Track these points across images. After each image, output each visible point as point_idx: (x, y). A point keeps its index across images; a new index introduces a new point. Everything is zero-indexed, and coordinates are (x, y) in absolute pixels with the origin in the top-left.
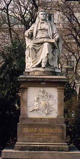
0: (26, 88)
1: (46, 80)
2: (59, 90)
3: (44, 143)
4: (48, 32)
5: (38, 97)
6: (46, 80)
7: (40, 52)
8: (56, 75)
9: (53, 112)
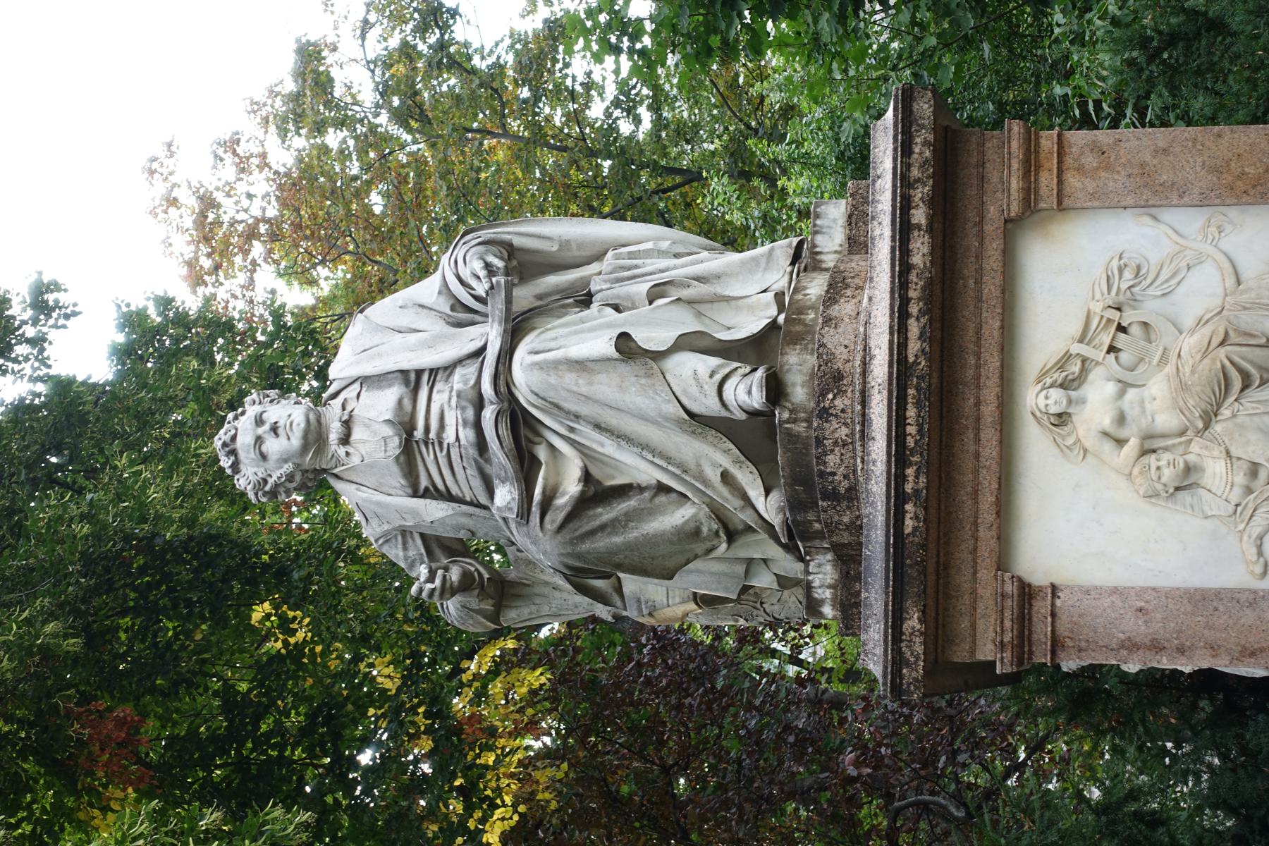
0: (1027, 592)
1: (914, 347)
4: (434, 372)
7: (608, 447)
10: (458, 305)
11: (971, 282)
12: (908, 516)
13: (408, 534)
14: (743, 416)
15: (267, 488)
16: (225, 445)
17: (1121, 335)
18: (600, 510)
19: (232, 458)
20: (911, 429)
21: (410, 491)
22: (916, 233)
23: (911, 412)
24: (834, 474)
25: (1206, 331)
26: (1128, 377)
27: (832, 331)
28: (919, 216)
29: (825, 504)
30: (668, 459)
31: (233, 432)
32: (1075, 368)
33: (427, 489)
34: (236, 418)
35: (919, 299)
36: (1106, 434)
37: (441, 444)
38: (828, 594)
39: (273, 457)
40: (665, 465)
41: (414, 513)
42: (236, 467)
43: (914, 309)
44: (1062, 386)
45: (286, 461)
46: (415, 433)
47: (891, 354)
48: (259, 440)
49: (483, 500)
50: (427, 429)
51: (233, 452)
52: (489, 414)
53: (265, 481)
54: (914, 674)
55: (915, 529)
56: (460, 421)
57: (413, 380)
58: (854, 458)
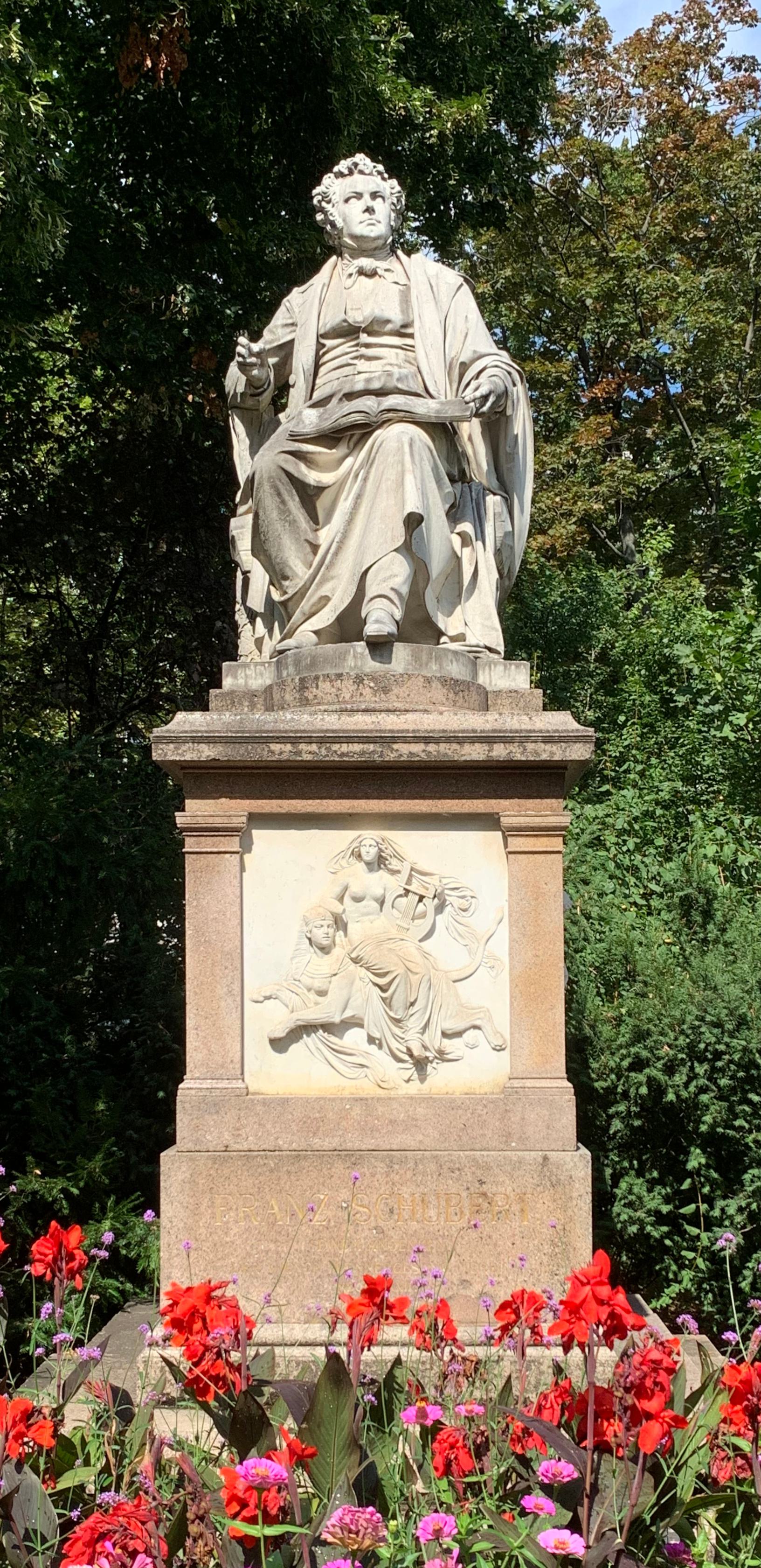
5: (338, 908)
7: (344, 506)
11: (454, 789)
12: (282, 746)
13: (293, 328)
14: (363, 615)
15: (324, 204)
16: (356, 165)
17: (417, 898)
18: (297, 499)
19: (346, 172)
21: (322, 331)
22: (487, 748)
23: (357, 747)
24: (317, 687)
25: (418, 958)
27: (421, 684)
28: (500, 752)
29: (297, 680)
30: (336, 554)
31: (367, 171)
33: (324, 346)
34: (379, 173)
35: (438, 752)
36: (346, 889)
37: (356, 358)
39: (346, 208)
40: (332, 551)
42: (340, 175)
43: (432, 748)
44: (380, 857)
45: (344, 220)
46: (365, 335)
47: (398, 732)
48: (359, 196)
49: (317, 396)
50: (367, 346)
51: (351, 173)
52: (369, 404)
53: (329, 202)
54: (169, 753)
55: (273, 752)
56: (373, 375)
58: (329, 703)
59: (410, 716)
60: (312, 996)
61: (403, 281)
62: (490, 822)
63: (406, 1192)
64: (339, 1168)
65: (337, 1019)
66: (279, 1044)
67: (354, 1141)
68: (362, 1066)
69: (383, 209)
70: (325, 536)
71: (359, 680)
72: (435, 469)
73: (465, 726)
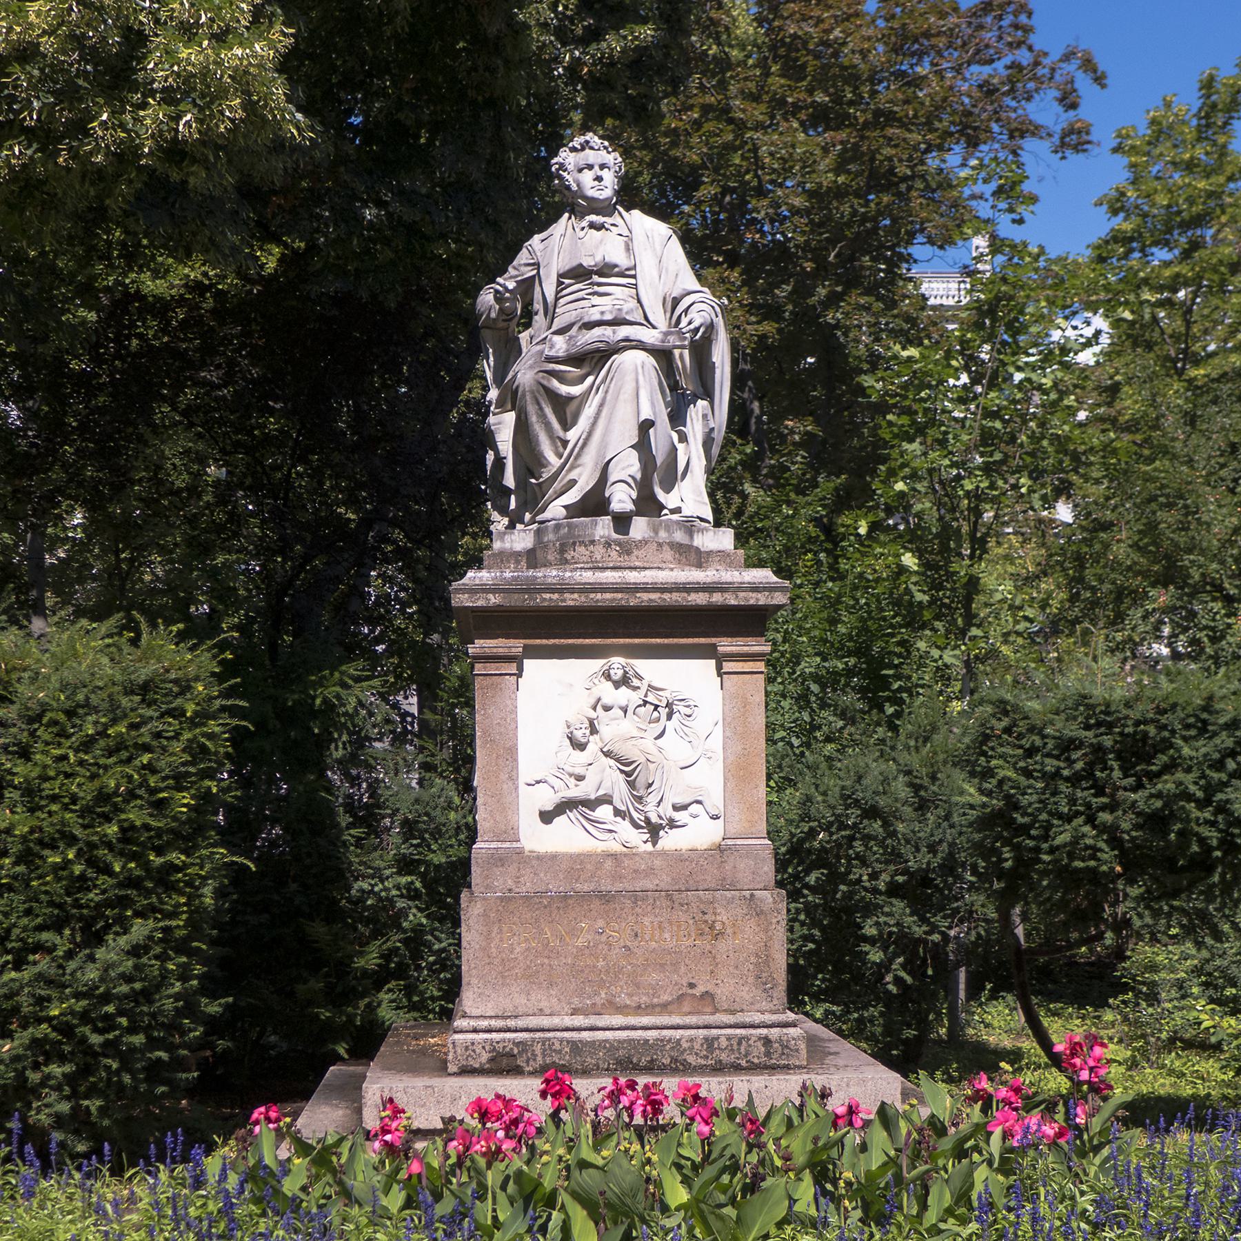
1: (645, 596)
2: (728, 666)
3: (646, 1020)
5: (593, 715)
6: (645, 596)
7: (588, 412)
8: (699, 565)
9: (694, 808)
10: (676, 301)
16: (587, 142)
20: (599, 596)
26: (630, 712)
28: (717, 598)
32: (636, 682)
38: (507, 545)
41: (548, 276)
42: (574, 150)
43: (666, 596)
48: (590, 167)
50: (600, 285)
51: (583, 149)
57: (628, 273)
59: (648, 573)
60: (572, 780)
61: (626, 233)
62: (708, 652)
63: (647, 921)
64: (596, 904)
65: (593, 797)
66: (547, 817)
67: (606, 885)
68: (611, 831)
69: (609, 177)
70: (572, 435)
71: (608, 544)
72: (660, 384)
73: (691, 579)
